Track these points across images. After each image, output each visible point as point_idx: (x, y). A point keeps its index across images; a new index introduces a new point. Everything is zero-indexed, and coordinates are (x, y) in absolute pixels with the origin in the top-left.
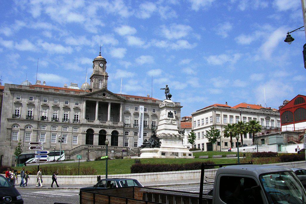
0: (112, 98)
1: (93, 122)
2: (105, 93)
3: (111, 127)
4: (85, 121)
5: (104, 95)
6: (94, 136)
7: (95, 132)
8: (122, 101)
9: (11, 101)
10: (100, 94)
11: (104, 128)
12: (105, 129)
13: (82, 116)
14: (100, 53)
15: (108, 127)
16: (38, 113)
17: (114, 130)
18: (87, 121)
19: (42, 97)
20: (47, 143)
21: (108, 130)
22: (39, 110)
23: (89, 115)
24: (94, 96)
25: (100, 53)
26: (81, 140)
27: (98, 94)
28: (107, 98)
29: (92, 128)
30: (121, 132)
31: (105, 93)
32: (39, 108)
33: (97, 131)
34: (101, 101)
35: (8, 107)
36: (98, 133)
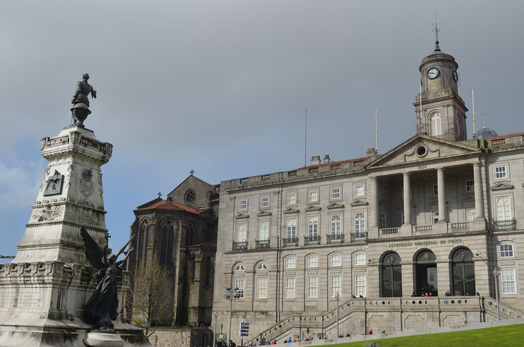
0: (443, 155)
1: (395, 231)
2: (421, 145)
3: (447, 239)
4: (374, 233)
5: (421, 151)
6: (403, 267)
7: (403, 260)
8: (474, 156)
9: (231, 215)
10: (410, 152)
11: (427, 243)
12: (429, 247)
13: (369, 220)
14: (437, 43)
15: (438, 240)
16: (279, 230)
17: (456, 245)
18: (381, 232)
19: (284, 193)
20: (298, 300)
21: (438, 249)
22: (279, 224)
23: (389, 214)
24: (392, 162)
25: (437, 43)
26: (367, 285)
27: (406, 153)
28: (431, 156)
29: (394, 249)
30: (477, 246)
31: (421, 145)
32: (279, 220)
33: (406, 254)
34: (416, 169)
35: (226, 229)
36: (411, 260)
